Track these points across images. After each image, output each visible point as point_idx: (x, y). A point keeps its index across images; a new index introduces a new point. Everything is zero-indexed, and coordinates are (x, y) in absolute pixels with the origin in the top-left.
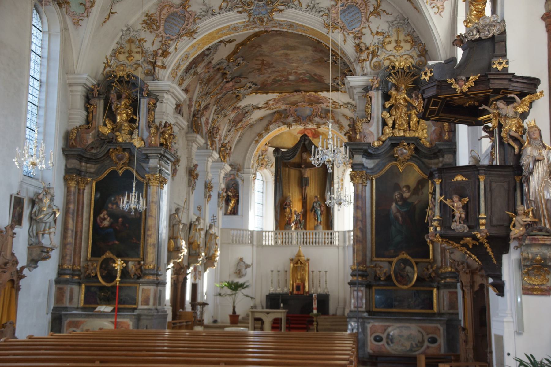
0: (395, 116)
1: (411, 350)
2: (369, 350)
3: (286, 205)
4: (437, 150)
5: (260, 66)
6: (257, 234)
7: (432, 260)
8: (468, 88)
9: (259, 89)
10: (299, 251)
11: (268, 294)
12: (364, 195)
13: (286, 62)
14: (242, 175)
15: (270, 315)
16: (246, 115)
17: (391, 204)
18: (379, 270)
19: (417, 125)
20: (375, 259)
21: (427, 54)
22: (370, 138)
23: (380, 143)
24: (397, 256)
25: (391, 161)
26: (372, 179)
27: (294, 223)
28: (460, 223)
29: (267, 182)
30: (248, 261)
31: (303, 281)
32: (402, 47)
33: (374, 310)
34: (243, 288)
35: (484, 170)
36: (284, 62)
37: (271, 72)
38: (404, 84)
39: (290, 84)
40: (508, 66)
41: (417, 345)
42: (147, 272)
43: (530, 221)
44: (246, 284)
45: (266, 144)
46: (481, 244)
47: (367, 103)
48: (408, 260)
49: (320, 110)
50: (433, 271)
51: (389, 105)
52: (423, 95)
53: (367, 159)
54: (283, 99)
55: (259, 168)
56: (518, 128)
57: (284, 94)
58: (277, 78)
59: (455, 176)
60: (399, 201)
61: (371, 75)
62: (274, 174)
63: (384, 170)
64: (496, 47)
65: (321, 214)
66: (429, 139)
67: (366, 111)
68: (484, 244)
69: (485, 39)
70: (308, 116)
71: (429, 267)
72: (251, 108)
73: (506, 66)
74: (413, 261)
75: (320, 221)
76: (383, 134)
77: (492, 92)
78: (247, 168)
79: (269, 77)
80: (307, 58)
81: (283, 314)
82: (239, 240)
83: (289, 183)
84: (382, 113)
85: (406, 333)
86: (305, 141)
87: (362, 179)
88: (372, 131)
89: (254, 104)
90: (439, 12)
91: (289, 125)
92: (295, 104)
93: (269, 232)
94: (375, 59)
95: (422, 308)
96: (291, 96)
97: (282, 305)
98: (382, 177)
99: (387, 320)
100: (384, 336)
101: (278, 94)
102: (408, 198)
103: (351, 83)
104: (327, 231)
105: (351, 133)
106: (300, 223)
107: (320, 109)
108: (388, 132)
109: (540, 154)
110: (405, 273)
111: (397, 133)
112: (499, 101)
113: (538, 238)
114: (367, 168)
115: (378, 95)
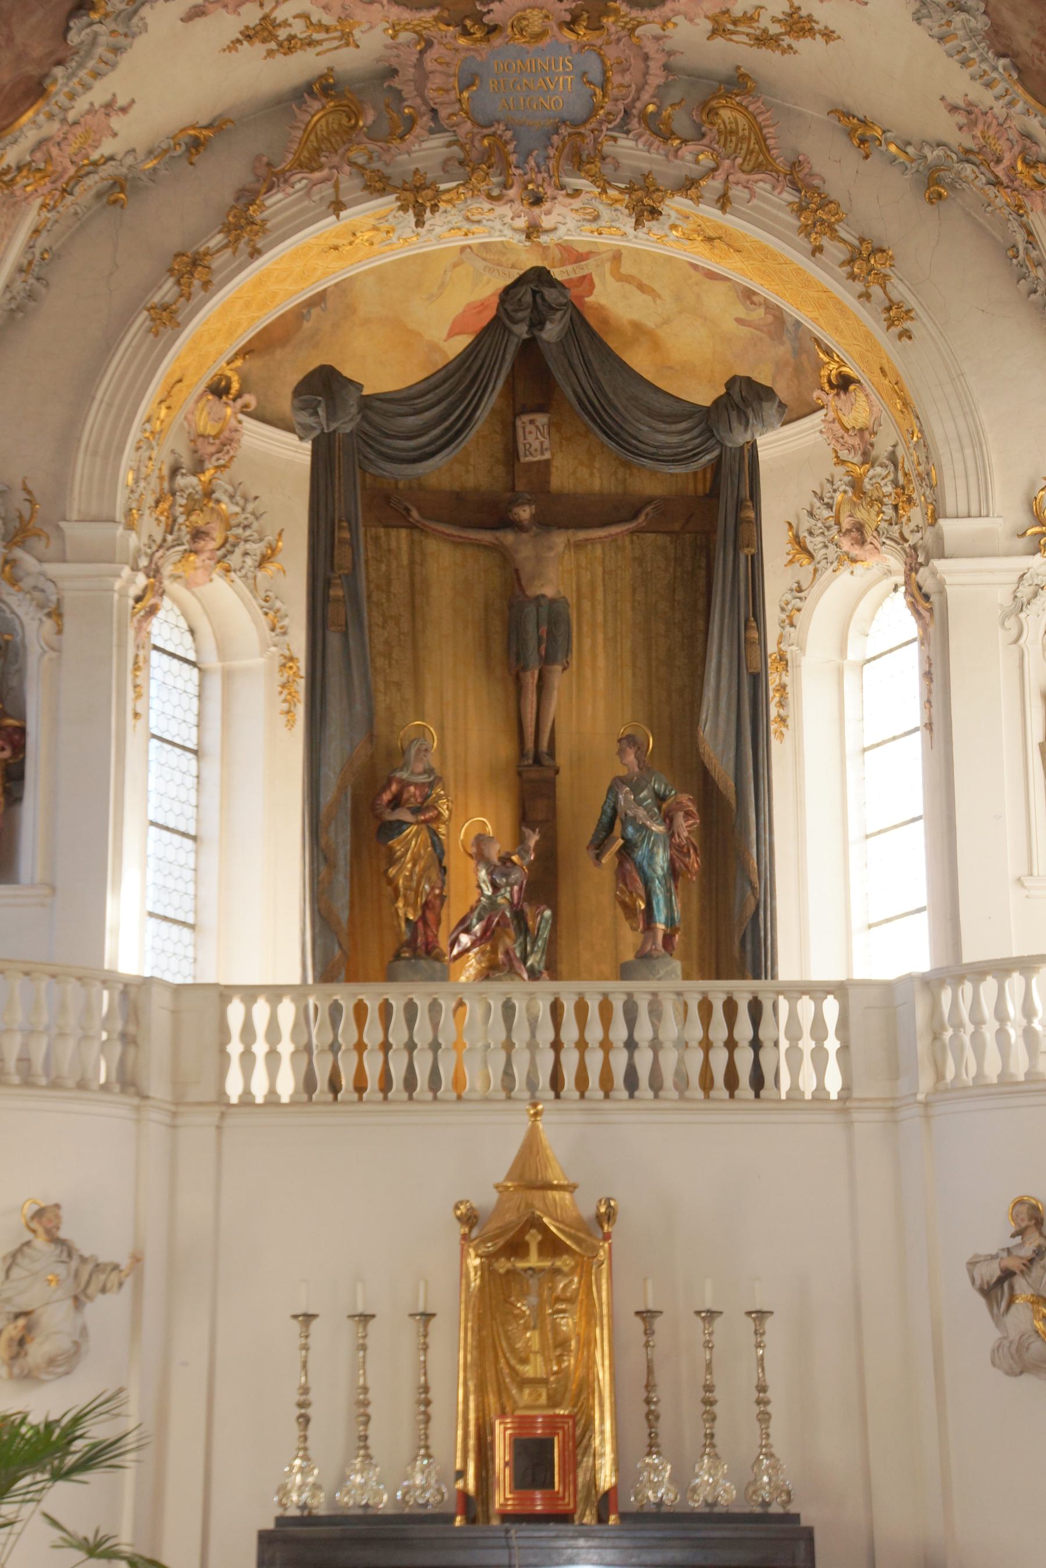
3: (396, 802)
6: (175, 1013)
10: (531, 1147)
14: (52, 569)
27: (477, 928)
29: (228, 676)
34: (59, 1475)
44: (97, 1431)
49: (657, 78)
65: (674, 873)
75: (670, 921)
78: (86, 519)
82: (25, 1060)
86: (537, 323)
106: (523, 929)
107: (655, 66)
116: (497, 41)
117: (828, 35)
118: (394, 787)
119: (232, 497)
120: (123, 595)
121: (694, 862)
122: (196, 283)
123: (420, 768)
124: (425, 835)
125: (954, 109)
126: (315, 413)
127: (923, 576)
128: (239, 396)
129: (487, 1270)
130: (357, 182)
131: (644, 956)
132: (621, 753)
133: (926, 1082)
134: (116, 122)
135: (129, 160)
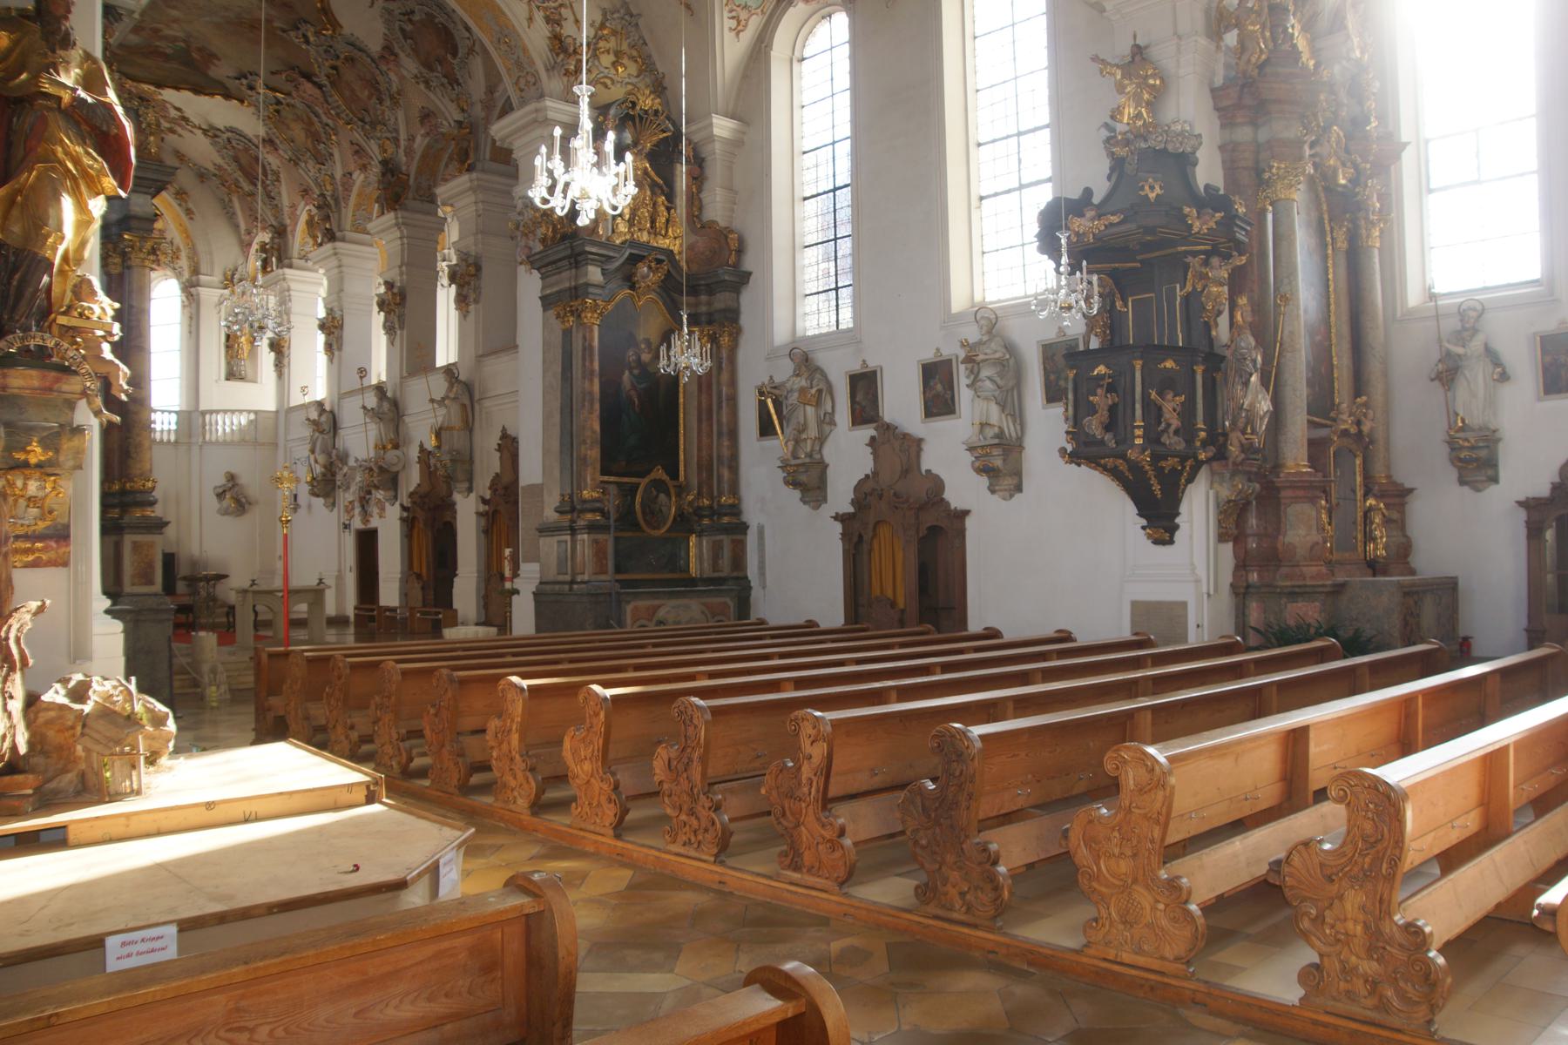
42: (139, 497)
48: (663, 482)
59: (1164, 360)
76: (613, 231)
90: (738, 32)
117: (180, 136)
125: (215, 164)
127: (192, 290)
133: (201, 440)
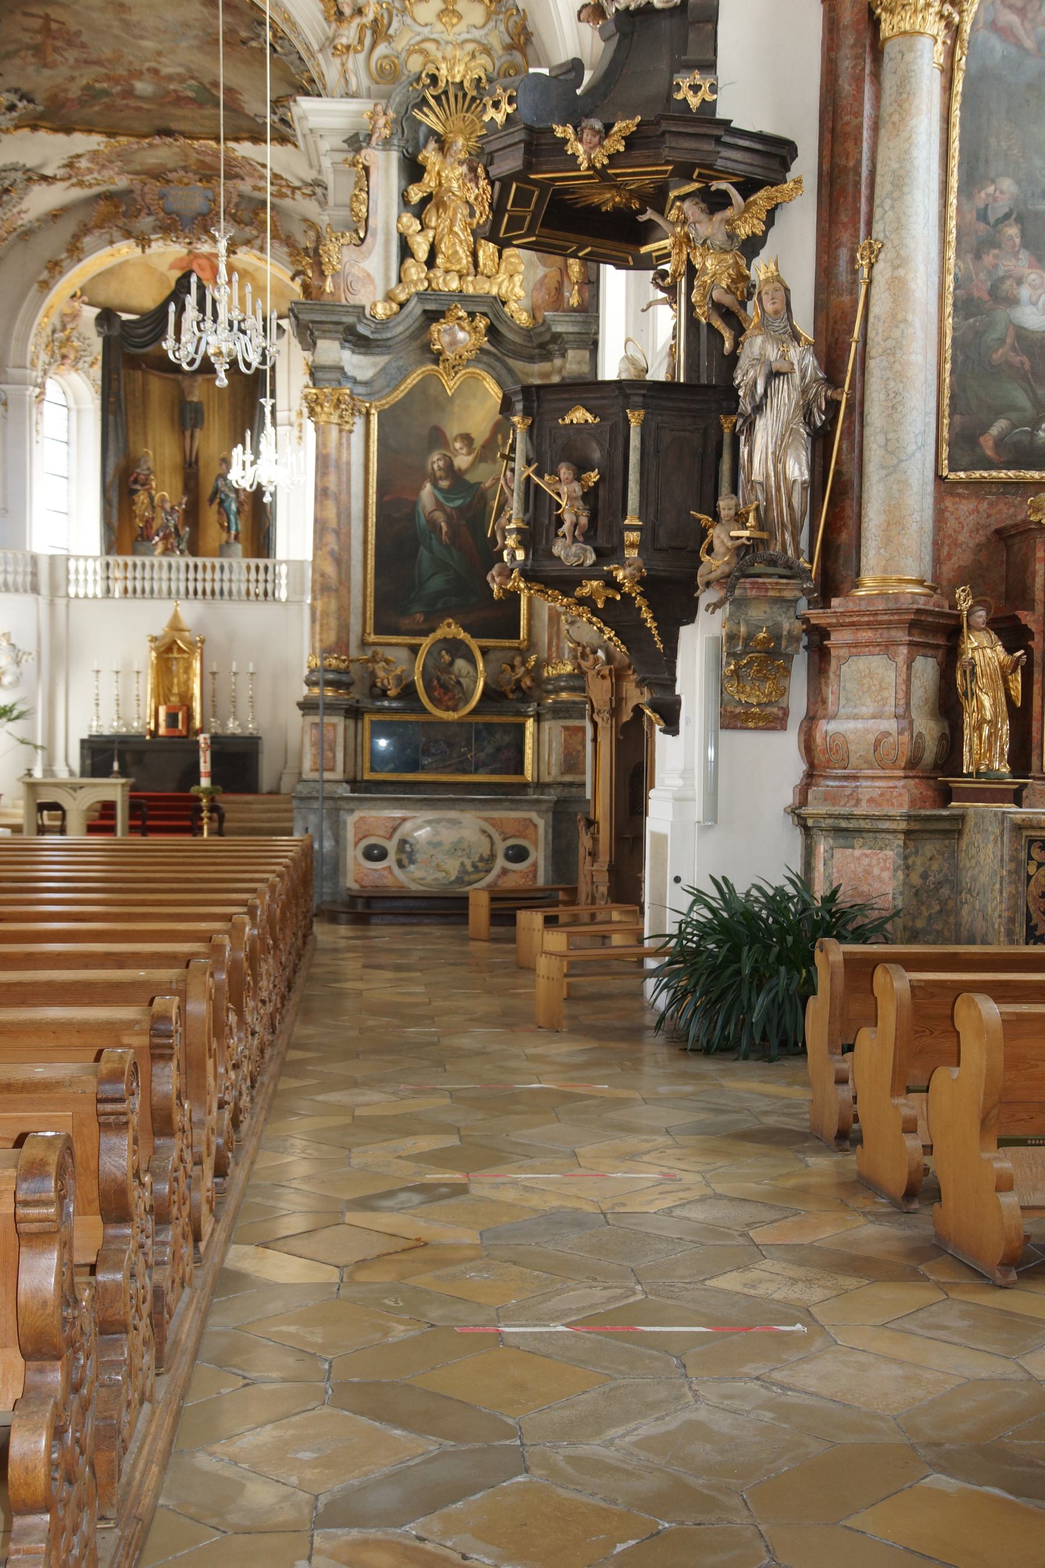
0: (435, 229)
1: (460, 881)
2: (350, 882)
3: (136, 481)
4: (547, 337)
5: (39, 39)
7: (526, 643)
8: (609, 157)
9: (42, 116)
10: (176, 617)
11: (85, 737)
12: (344, 459)
13: (124, 35)
15: (81, 793)
16: (5, 198)
17: (420, 488)
18: (385, 669)
19: (497, 259)
20: (372, 638)
21: (532, 43)
22: (363, 292)
23: (391, 309)
24: (433, 630)
25: (422, 363)
26: (368, 414)
27: (161, 534)
28: (575, 540)
29: (79, 411)
30: (26, 643)
31: (186, 701)
32: (460, 17)
33: (368, 776)
34: (10, 720)
35: (644, 396)
36: (116, 31)
37: (77, 61)
38: (461, 132)
39: (138, 109)
40: (715, 97)
41: (474, 866)
43: (748, 539)
45: (73, 296)
46: (627, 597)
47: (356, 183)
50: (528, 672)
51: (421, 195)
52: (489, 169)
53: (353, 352)
54: (122, 155)
55: (54, 367)
56: (733, 281)
57: (123, 140)
58: (97, 85)
59: (566, 411)
60: (441, 478)
61: (369, 97)
62: (100, 391)
63: (402, 387)
64: (691, 36)
65: (238, 512)
66: (526, 303)
67: (352, 210)
68: (635, 598)
69: (663, 10)
70: (200, 214)
71: (517, 661)
72: (19, 176)
73: (709, 98)
74: (474, 644)
75: (237, 530)
76: (400, 281)
77: (673, 174)
79: (72, 79)
80: (189, 26)
81: (119, 789)
83: (145, 416)
84: (399, 218)
85: (448, 836)
87: (338, 412)
88: (371, 272)
89: (28, 166)
91: (143, 242)
92: (158, 174)
93: (86, 558)
94: (382, 49)
95: (493, 772)
96: (144, 149)
97: (116, 766)
98: (394, 407)
99: (400, 803)
100: (391, 846)
101: (105, 139)
102: (467, 471)
103: (310, 118)
104: (253, 562)
105: (310, 273)
107: (234, 196)
108: (415, 278)
109: (783, 356)
110: (453, 677)
111: (441, 280)
112: (690, 199)
113: (764, 583)
114: (355, 381)
115: (388, 160)
116: (171, 184)
118: (135, 475)
119: (78, 339)
120: (30, 396)
121: (247, 508)
122: (57, 272)
123: (145, 467)
124: (146, 494)
126: (102, 327)
128: (80, 297)
129: (157, 658)
130: (119, 233)
131: (227, 543)
132: (221, 465)
134: (23, 215)
135: (29, 225)
